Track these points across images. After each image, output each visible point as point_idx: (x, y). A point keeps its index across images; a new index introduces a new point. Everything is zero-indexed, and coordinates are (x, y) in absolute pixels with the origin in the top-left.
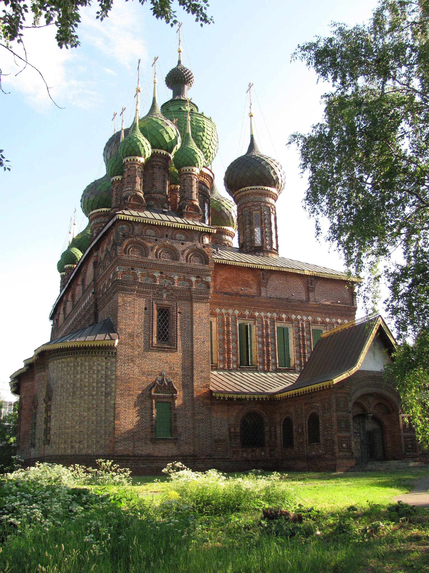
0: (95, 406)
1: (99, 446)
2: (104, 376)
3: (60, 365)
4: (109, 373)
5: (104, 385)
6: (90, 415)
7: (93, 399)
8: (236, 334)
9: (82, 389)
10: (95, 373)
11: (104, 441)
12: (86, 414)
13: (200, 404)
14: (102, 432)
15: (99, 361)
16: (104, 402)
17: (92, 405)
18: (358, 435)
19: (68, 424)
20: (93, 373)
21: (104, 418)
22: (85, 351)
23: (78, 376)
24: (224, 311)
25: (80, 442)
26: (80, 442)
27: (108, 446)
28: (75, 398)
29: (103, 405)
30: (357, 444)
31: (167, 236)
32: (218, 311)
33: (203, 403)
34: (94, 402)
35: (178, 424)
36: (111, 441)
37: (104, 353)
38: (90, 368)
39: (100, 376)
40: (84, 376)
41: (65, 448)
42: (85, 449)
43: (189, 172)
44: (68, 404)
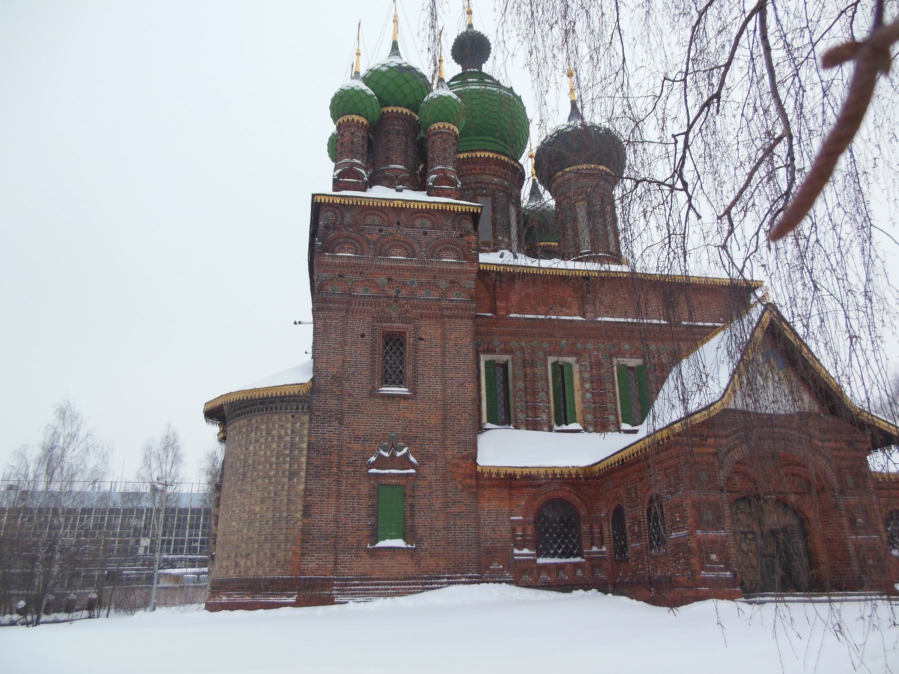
0: (272, 494)
1: (275, 562)
2: (288, 446)
4: (297, 439)
5: (288, 459)
6: (265, 509)
7: (270, 483)
8: (547, 379)
9: (254, 468)
10: (275, 441)
11: (283, 553)
12: (258, 509)
13: (457, 487)
14: (282, 537)
15: (282, 421)
16: (286, 487)
17: (269, 493)
18: (750, 536)
19: (234, 526)
20: (273, 441)
21: (285, 515)
22: (261, 406)
24: (523, 344)
26: (247, 555)
27: (289, 562)
28: (245, 482)
29: (285, 493)
30: (751, 555)
31: (398, 224)
32: (514, 344)
33: (462, 485)
34: (271, 488)
35: (418, 521)
36: (295, 553)
37: (289, 408)
39: (282, 445)
40: (260, 447)
41: (227, 566)
42: (253, 567)
43: (439, 130)
44: (237, 494)
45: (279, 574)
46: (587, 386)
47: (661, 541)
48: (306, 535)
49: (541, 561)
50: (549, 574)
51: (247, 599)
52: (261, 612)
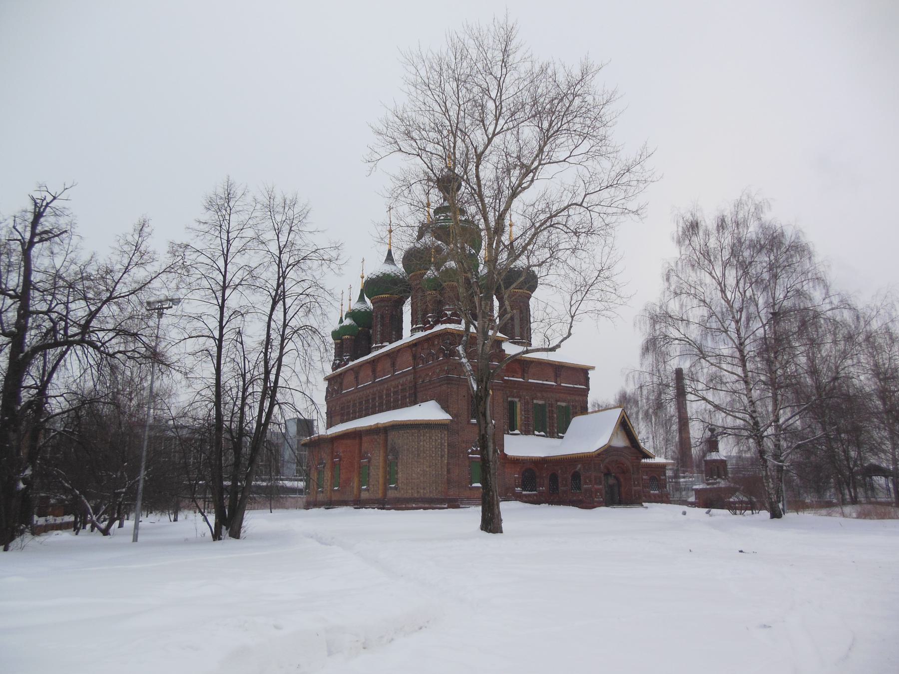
3: (405, 435)
12: (428, 469)
14: (439, 482)
23: (422, 443)
25: (424, 489)
38: (430, 438)
45: (439, 496)
46: (523, 413)
47: (579, 489)
48: (449, 482)
49: (524, 493)
50: (526, 498)
51: (427, 506)
52: (437, 510)
